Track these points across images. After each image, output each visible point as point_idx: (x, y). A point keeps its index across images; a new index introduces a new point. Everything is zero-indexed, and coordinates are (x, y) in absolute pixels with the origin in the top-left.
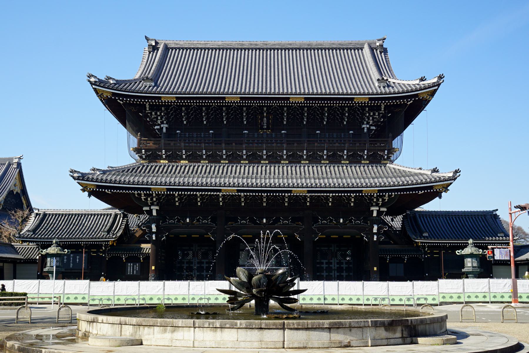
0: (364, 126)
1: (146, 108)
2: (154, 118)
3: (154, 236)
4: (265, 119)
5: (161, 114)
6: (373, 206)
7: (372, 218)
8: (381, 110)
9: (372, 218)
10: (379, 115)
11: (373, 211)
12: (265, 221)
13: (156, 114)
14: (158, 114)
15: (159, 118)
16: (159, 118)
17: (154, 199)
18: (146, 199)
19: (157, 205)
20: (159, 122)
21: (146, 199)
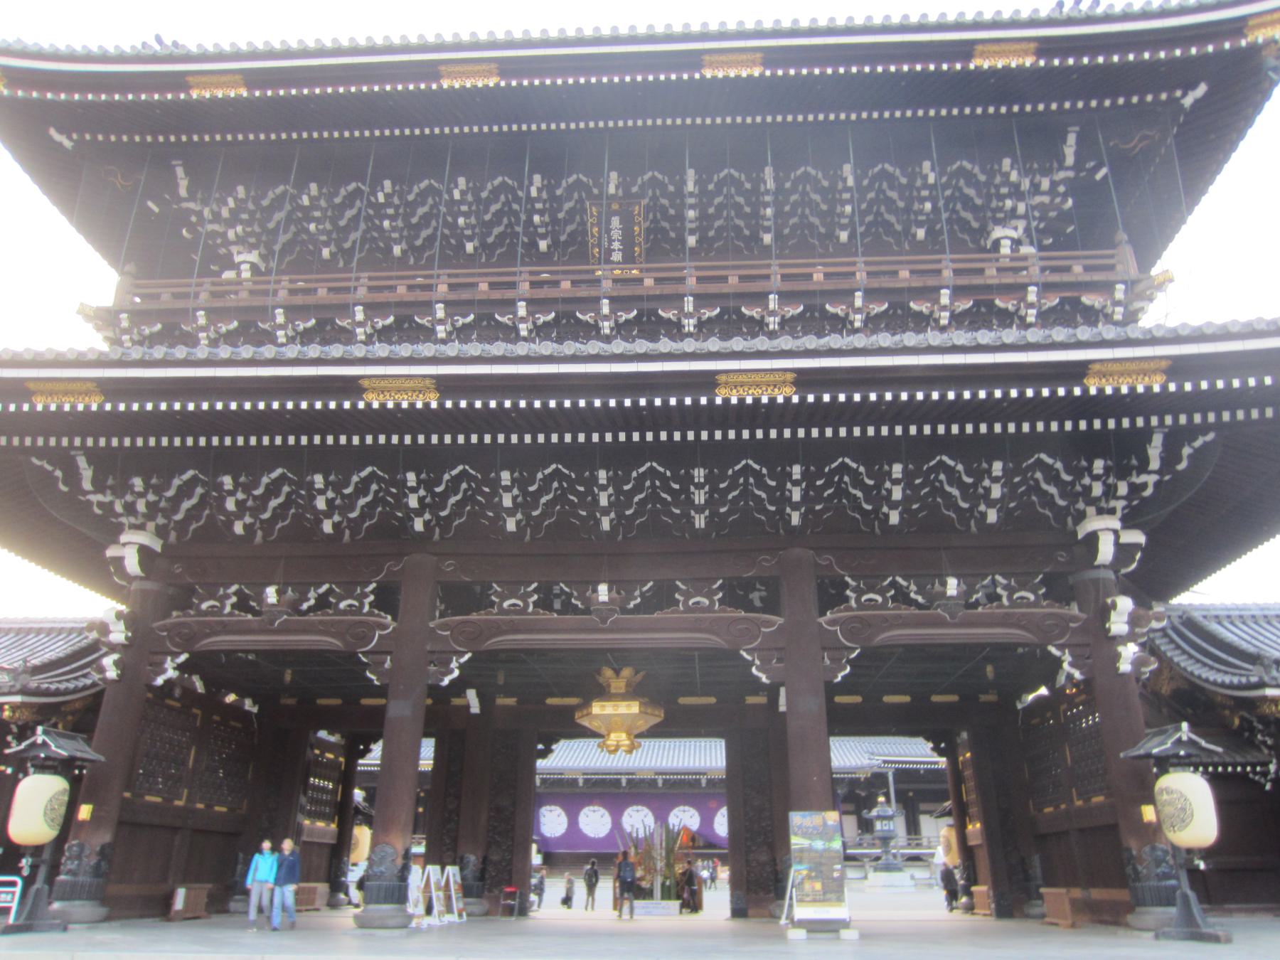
4: (615, 222)
6: (1081, 516)
7: (1093, 574)
9: (1093, 574)
11: (1093, 538)
12: (603, 592)
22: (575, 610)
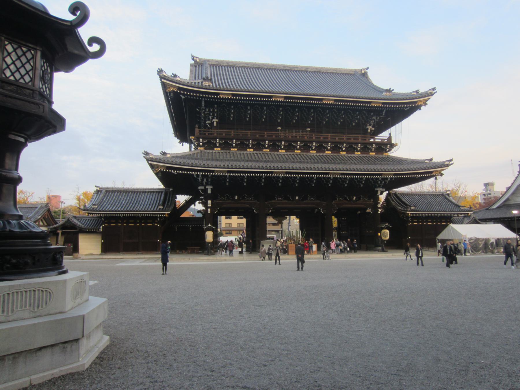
0: (368, 127)
1: (202, 105)
2: (207, 114)
3: (209, 210)
5: (214, 110)
6: (376, 187)
8: (382, 115)
10: (380, 118)
11: (377, 191)
13: (209, 110)
14: (211, 110)
15: (211, 114)
16: (211, 114)
17: (209, 180)
18: (202, 180)
19: (211, 185)
20: (211, 117)
21: (202, 180)
22: (290, 200)
